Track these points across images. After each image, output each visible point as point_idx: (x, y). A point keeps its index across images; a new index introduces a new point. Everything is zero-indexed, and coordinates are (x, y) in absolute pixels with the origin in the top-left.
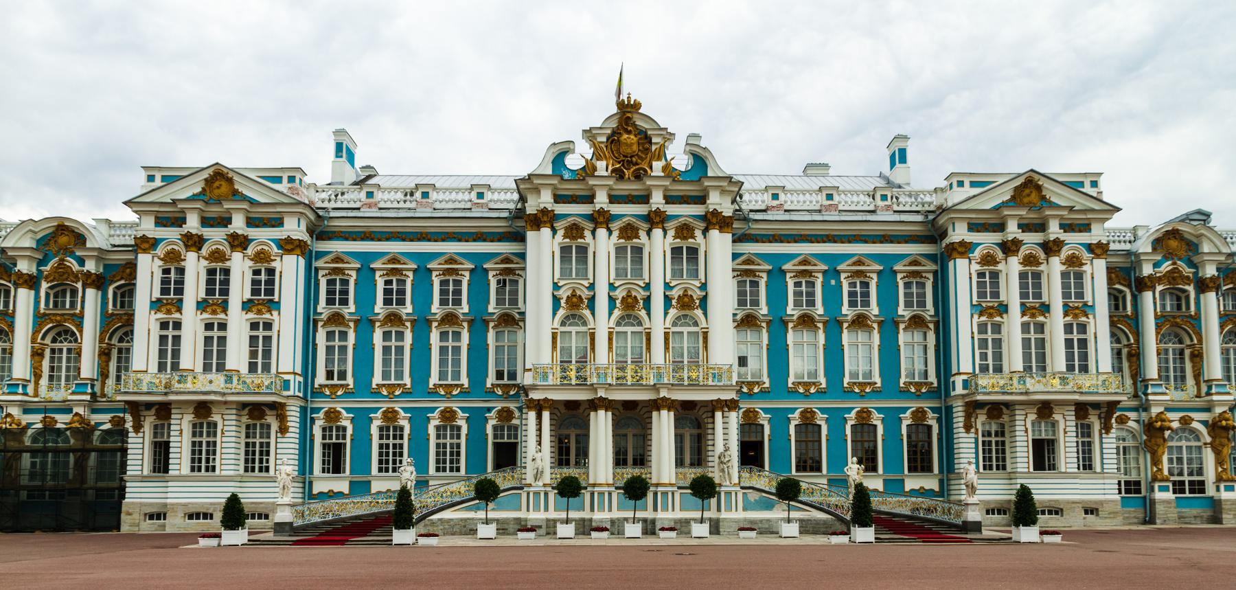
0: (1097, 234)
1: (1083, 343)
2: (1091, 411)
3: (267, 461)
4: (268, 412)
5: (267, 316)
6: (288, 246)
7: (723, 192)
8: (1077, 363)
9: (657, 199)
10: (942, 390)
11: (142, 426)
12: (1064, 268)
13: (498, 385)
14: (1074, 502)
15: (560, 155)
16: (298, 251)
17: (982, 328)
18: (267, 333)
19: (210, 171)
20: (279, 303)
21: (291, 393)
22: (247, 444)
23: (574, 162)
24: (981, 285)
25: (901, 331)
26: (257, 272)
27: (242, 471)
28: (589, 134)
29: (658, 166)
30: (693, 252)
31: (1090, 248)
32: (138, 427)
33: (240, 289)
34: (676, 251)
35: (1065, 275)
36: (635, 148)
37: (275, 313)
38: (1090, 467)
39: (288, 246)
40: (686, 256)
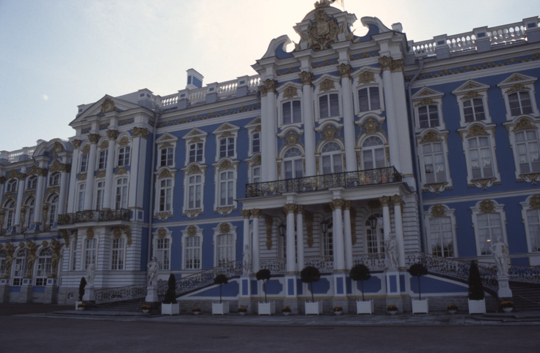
5: (125, 175)
7: (390, 42)
9: (343, 57)
15: (278, 45)
16: (140, 135)
18: (125, 185)
20: (130, 166)
22: (114, 251)
23: (290, 48)
26: (122, 151)
27: (110, 268)
28: (298, 28)
29: (341, 37)
30: (375, 91)
32: (68, 245)
33: (110, 163)
34: (362, 93)
36: (326, 28)
37: (128, 172)
40: (369, 96)
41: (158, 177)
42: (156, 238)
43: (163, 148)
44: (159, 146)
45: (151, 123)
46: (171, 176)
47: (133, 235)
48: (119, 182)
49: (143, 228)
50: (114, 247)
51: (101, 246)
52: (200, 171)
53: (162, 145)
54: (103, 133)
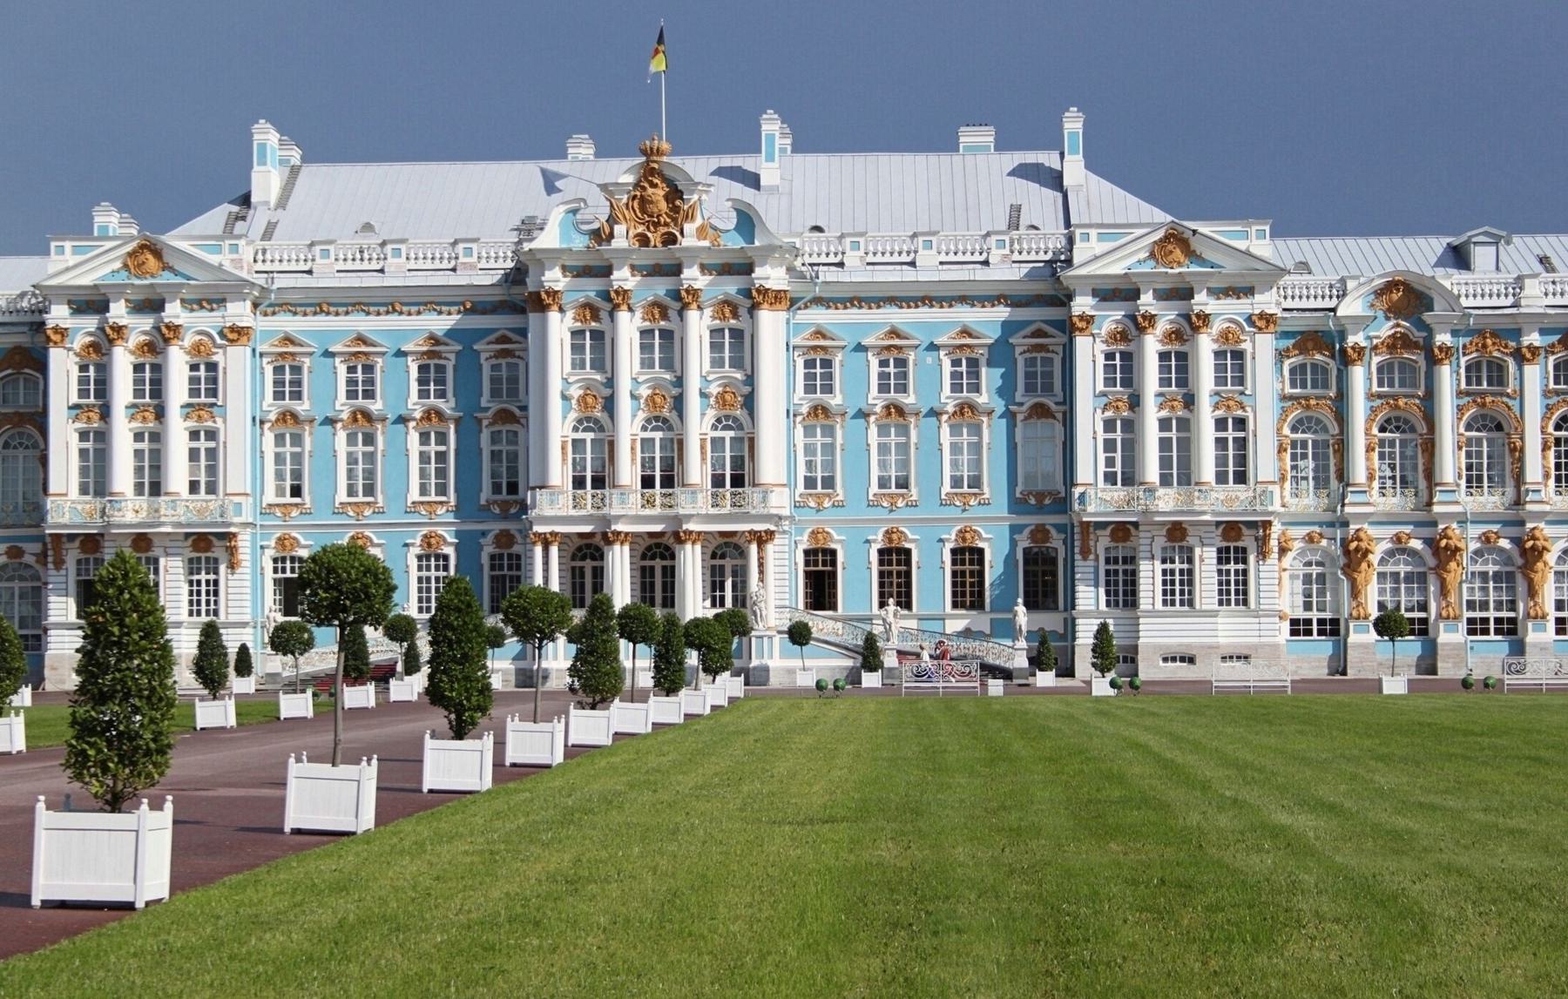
0: (1266, 302)
1: (1241, 444)
2: (1245, 530)
3: (216, 602)
6: (236, 334)
8: (1231, 469)
10: (1062, 503)
11: (63, 562)
12: (1215, 347)
13: (495, 502)
14: (1211, 647)
17: (1109, 425)
24: (1109, 369)
25: (1019, 424)
26: (194, 367)
31: (1250, 320)
35: (1219, 354)
37: (219, 420)
38: (1245, 603)
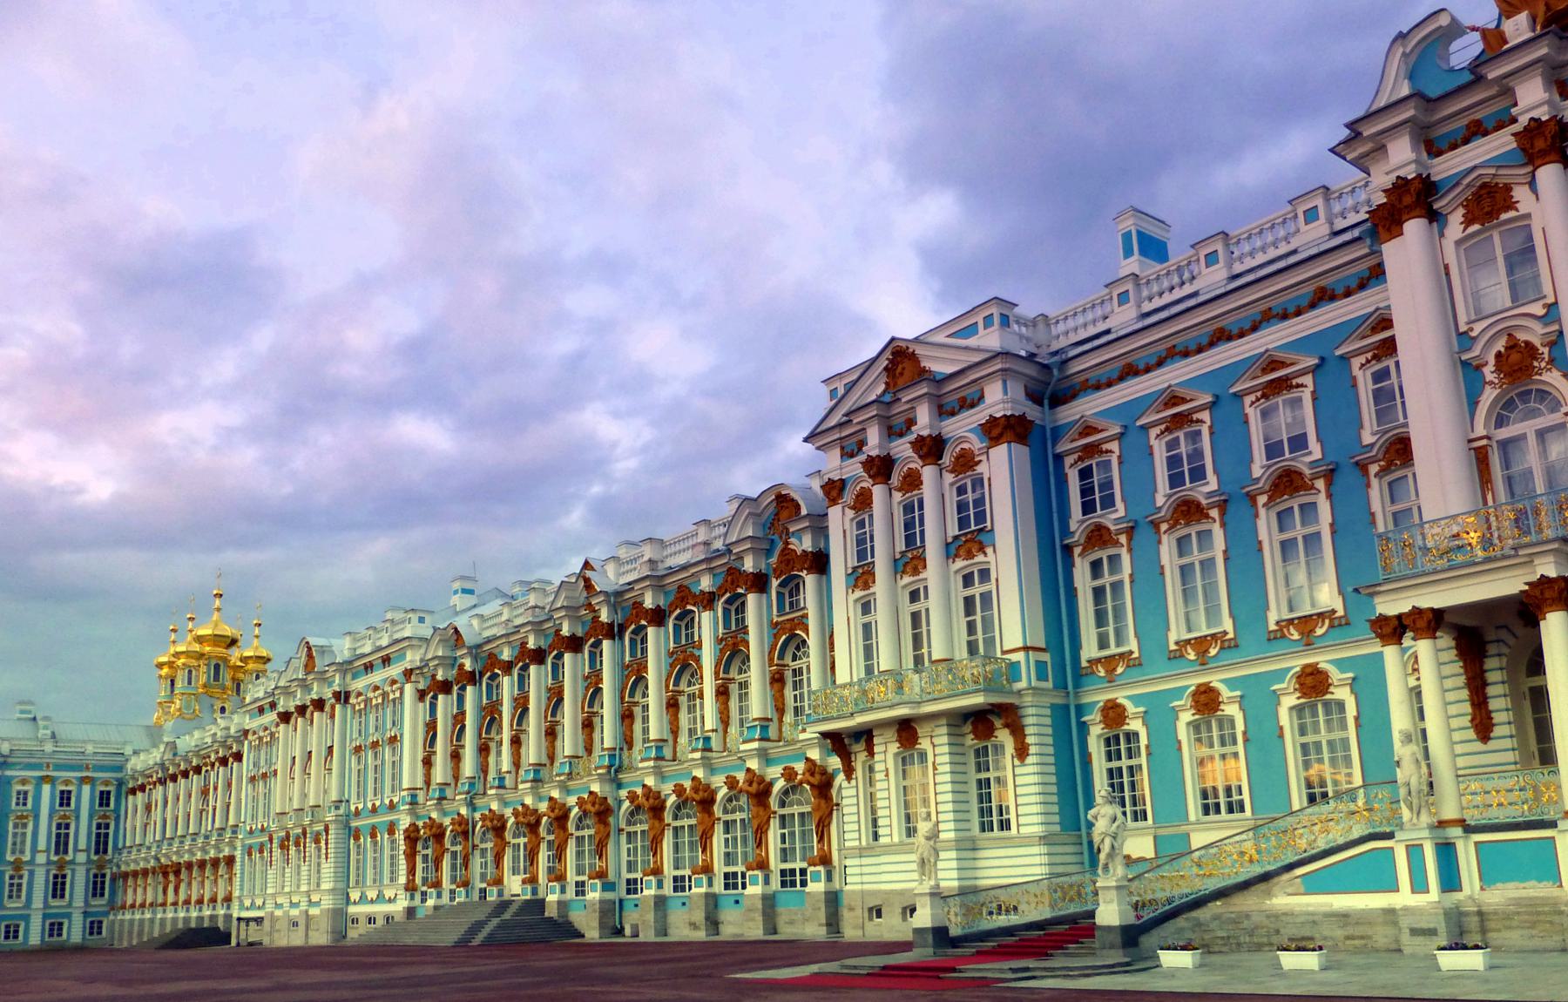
4: (998, 723)
5: (980, 558)
6: (996, 431)
16: (1009, 435)
19: (888, 354)
20: (992, 530)
21: (1023, 684)
22: (979, 781)
26: (961, 490)
32: (849, 772)
37: (989, 550)
39: (996, 431)
41: (1077, 551)
42: (1096, 731)
43: (1082, 465)
44: (1069, 460)
45: (1035, 397)
46: (1117, 543)
47: (1029, 730)
48: (968, 580)
49: (1053, 707)
50: (979, 771)
51: (941, 769)
52: (1207, 516)
53: (1076, 456)
54: (902, 449)
